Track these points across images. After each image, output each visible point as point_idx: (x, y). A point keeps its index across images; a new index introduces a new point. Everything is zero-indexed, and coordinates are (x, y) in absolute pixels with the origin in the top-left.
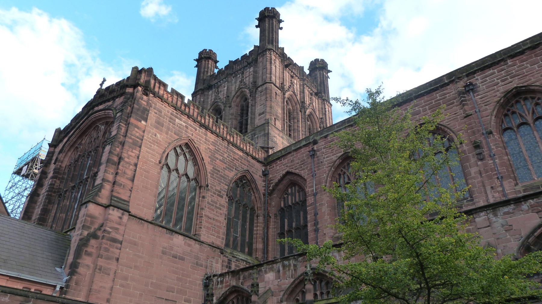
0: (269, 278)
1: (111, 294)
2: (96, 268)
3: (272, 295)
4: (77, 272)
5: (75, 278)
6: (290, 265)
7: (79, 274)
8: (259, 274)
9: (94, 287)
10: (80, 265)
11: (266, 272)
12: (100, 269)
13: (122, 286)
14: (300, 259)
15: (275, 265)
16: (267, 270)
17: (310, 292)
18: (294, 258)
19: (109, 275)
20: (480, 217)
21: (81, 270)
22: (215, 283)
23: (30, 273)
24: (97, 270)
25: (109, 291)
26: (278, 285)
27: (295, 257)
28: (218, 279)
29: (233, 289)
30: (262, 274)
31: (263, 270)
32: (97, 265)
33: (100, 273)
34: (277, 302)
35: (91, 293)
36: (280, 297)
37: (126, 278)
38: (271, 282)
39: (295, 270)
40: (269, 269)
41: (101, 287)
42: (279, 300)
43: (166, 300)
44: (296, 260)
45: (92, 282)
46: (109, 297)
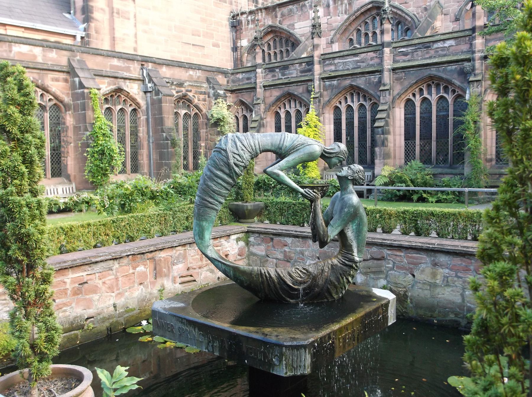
1: (136, 42)
2: (113, 12)
4: (93, 18)
5: (93, 25)
7: (97, 20)
8: (302, 10)
9: (117, 35)
10: (94, 9)
12: (118, 13)
13: (146, 32)
17: (388, 33)
19: (129, 19)
21: (96, 15)
22: (245, 23)
23: (43, 22)
24: (115, 14)
25: (134, 39)
28: (247, 17)
29: (270, 30)
30: (306, 10)
31: (307, 5)
32: (113, 8)
33: (119, 18)
35: (116, 42)
36: (330, 37)
37: (146, 23)
41: (124, 34)
43: (193, 45)
45: (112, 29)
46: (134, 45)
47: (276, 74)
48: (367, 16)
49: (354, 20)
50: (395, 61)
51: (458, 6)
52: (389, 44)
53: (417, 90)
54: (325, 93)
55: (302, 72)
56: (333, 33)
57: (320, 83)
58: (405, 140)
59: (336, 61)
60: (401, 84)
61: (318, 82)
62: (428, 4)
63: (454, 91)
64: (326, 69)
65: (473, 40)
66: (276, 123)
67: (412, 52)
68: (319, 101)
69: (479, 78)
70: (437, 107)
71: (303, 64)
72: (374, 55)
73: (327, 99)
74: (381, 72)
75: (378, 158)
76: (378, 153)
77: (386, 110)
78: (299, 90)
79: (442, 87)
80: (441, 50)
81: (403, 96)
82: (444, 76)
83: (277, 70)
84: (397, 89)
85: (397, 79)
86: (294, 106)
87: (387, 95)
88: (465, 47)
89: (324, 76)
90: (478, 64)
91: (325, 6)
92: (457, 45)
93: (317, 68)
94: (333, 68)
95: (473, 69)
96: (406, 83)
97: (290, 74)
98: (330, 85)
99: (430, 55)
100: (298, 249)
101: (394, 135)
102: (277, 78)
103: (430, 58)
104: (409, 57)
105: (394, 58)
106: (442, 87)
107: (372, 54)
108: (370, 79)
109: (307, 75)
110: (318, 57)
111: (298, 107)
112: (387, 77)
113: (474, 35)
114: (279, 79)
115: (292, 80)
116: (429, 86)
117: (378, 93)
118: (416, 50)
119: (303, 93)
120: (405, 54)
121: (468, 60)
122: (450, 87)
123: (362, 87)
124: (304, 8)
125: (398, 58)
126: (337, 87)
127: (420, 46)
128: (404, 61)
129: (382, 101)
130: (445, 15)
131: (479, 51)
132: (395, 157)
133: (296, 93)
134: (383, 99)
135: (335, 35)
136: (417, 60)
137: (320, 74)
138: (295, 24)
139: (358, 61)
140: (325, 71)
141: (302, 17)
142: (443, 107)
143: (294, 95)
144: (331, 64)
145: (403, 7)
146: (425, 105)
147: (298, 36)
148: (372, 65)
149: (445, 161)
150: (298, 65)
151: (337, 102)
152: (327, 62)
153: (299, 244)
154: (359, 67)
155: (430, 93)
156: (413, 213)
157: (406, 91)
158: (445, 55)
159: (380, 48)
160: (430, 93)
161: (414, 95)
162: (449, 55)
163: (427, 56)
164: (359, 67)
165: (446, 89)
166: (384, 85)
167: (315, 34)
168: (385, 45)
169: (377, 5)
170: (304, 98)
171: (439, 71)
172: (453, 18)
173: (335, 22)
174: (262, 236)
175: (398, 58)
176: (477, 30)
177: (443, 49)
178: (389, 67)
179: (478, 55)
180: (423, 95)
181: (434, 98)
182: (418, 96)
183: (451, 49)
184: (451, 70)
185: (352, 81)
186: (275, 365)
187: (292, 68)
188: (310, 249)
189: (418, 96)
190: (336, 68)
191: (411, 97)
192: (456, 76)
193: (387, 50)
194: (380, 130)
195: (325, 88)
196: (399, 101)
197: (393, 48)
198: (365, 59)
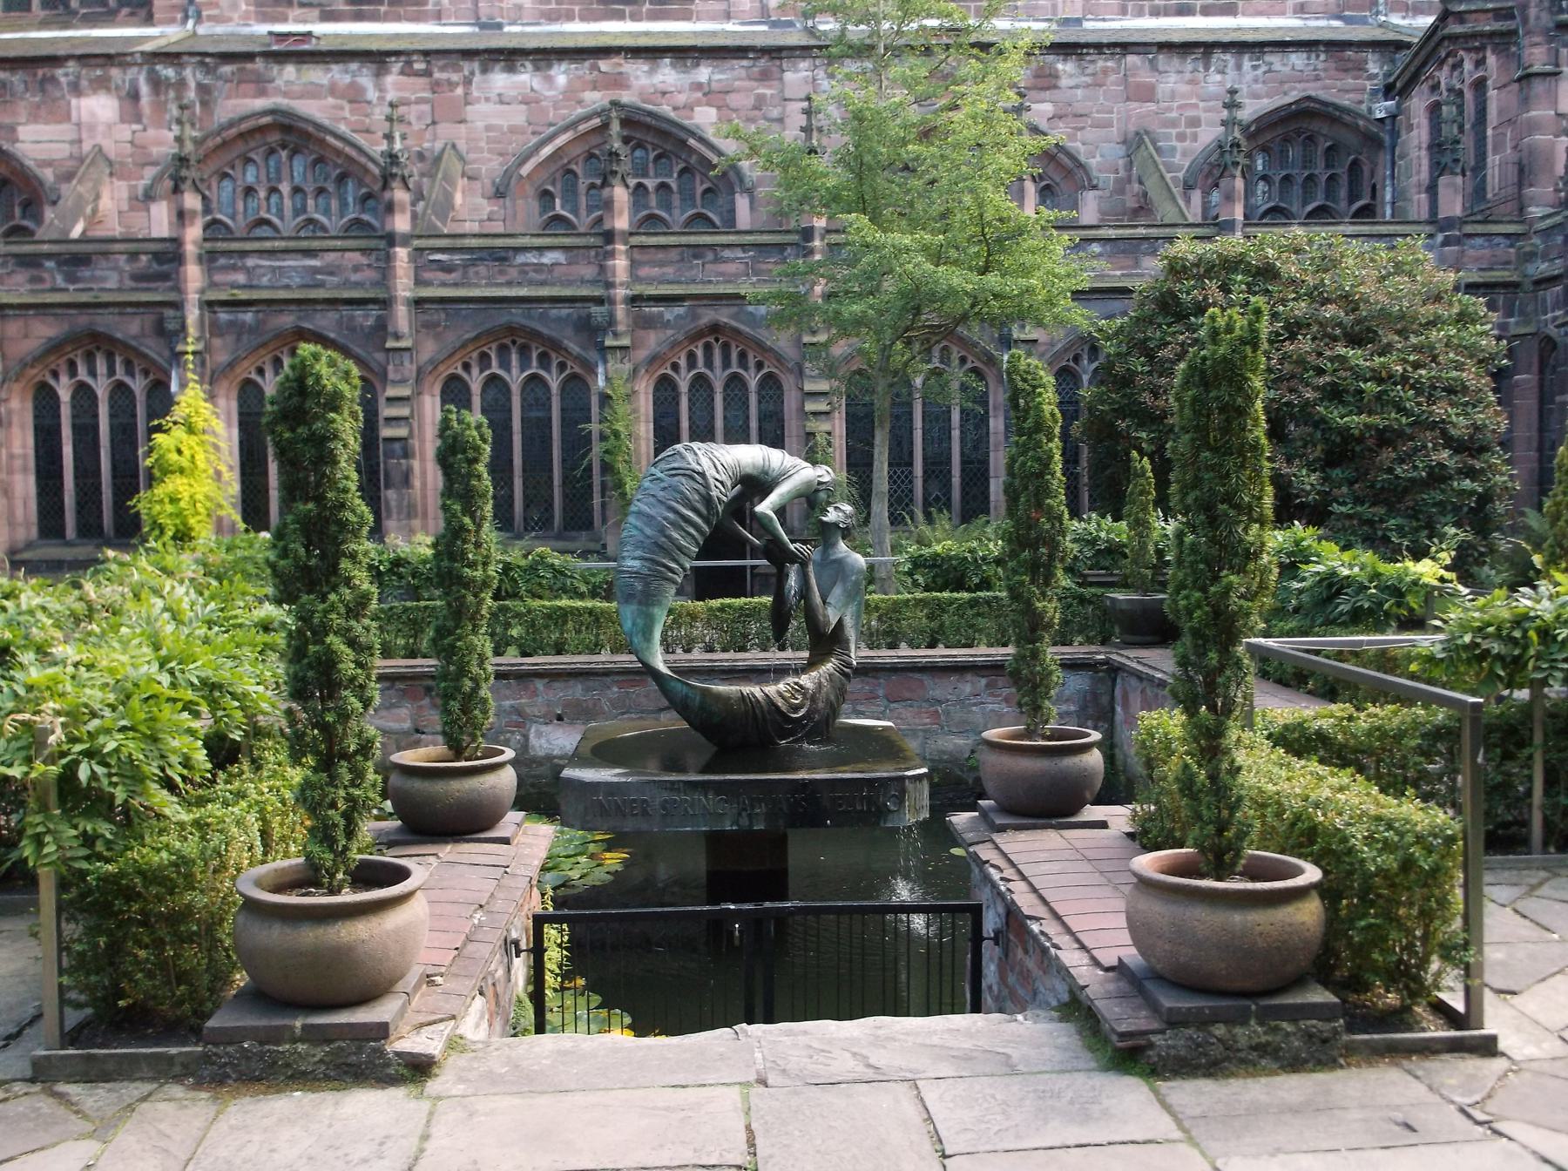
0: (93, 114)
3: (111, 174)
6: (181, 84)
11: (76, 89)
14: (227, 69)
15: (115, 72)
16: (84, 83)
17: (403, 211)
18: (202, 63)
20: (797, 71)
26: (131, 142)
27: (208, 60)
30: (58, 94)
31: (63, 80)
34: (130, 199)
36: (142, 184)
38: (101, 128)
39: (204, 104)
40: (91, 81)
42: (140, 192)
44: (208, 70)
47: (46, 275)
48: (252, 144)
49: (218, 148)
50: (419, 282)
51: (501, 164)
52: (406, 240)
53: (475, 355)
54: (217, 342)
55: (137, 277)
56: (150, 173)
57: (202, 316)
58: (890, 465)
59: (250, 262)
60: (437, 337)
61: (197, 312)
62: (426, 145)
63: (562, 366)
64: (218, 278)
65: (605, 258)
66: (36, 417)
67: (465, 267)
68: (203, 363)
69: (626, 342)
70: (523, 400)
71: (144, 258)
72: (364, 261)
73: (223, 358)
74: (386, 303)
75: (395, 516)
76: (393, 504)
77: (407, 399)
78: (131, 328)
79: (534, 355)
80: (535, 271)
81: (441, 368)
82: (545, 331)
83: (50, 264)
84: (429, 350)
85: (429, 326)
86: (105, 371)
87: (407, 363)
88: (589, 272)
89: (213, 295)
90: (621, 311)
91: (123, 93)
92: (569, 264)
93: (193, 274)
94: (241, 278)
95: (612, 321)
96: (452, 338)
97: (93, 279)
98: (232, 324)
99: (507, 278)
100: (507, 703)
101: (423, 460)
102: (47, 286)
103: (509, 284)
104: (454, 276)
105: (416, 275)
106: (534, 355)
107: (356, 257)
108: (352, 318)
109: (156, 290)
110: (195, 243)
111: (120, 374)
112: (402, 317)
113: (609, 248)
114: (55, 290)
115: (106, 298)
116: (503, 351)
117: (380, 356)
118: (474, 262)
119: (143, 335)
120: (448, 268)
121: (599, 301)
122: (553, 355)
123: (332, 335)
124: (49, 87)
125: (427, 275)
126: (253, 330)
127: (484, 254)
128: (444, 284)
129: (391, 376)
130: (470, 178)
131: (622, 284)
132: (425, 515)
133: (119, 335)
134: (396, 371)
135: (157, 179)
136: (477, 285)
137: (202, 291)
138: (20, 129)
139: (316, 270)
140: (213, 285)
141: (43, 112)
142: (537, 400)
143: (112, 340)
144: (234, 268)
145: (360, 139)
146: (492, 393)
147: (30, 163)
148: (358, 285)
149: (545, 523)
150: (124, 257)
151: (253, 369)
152: (222, 261)
153: (508, 692)
154: (321, 285)
155: (505, 365)
156: (741, 608)
157: (450, 356)
158: (543, 283)
159: (382, 244)
160: (505, 365)
161: (467, 367)
162: (553, 284)
163: (501, 280)
164: (321, 285)
165: (544, 360)
166: (397, 337)
167: (189, 182)
168: (398, 239)
169: (286, 121)
170: (147, 351)
171: (530, 317)
172: (491, 190)
173: (159, 143)
174: (400, 685)
175: (427, 275)
176: (617, 238)
177: (539, 268)
178: (408, 294)
179: (620, 293)
180: (489, 366)
181: (515, 378)
182: (475, 371)
183: (557, 271)
184: (559, 319)
185: (300, 318)
186: (890, 811)
187: (104, 264)
188: (540, 699)
189: (475, 371)
190: (250, 279)
191: (460, 371)
192: (569, 331)
193: (402, 253)
194: (397, 446)
195: (216, 329)
196: (431, 378)
197: (416, 249)
198: (339, 267)
